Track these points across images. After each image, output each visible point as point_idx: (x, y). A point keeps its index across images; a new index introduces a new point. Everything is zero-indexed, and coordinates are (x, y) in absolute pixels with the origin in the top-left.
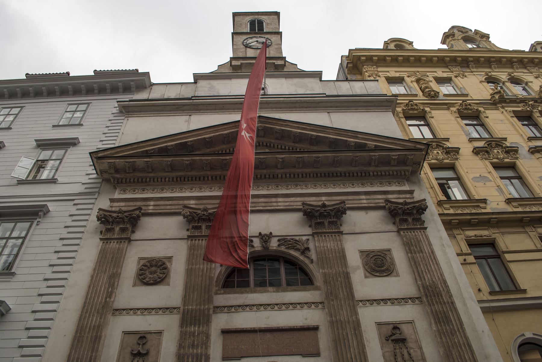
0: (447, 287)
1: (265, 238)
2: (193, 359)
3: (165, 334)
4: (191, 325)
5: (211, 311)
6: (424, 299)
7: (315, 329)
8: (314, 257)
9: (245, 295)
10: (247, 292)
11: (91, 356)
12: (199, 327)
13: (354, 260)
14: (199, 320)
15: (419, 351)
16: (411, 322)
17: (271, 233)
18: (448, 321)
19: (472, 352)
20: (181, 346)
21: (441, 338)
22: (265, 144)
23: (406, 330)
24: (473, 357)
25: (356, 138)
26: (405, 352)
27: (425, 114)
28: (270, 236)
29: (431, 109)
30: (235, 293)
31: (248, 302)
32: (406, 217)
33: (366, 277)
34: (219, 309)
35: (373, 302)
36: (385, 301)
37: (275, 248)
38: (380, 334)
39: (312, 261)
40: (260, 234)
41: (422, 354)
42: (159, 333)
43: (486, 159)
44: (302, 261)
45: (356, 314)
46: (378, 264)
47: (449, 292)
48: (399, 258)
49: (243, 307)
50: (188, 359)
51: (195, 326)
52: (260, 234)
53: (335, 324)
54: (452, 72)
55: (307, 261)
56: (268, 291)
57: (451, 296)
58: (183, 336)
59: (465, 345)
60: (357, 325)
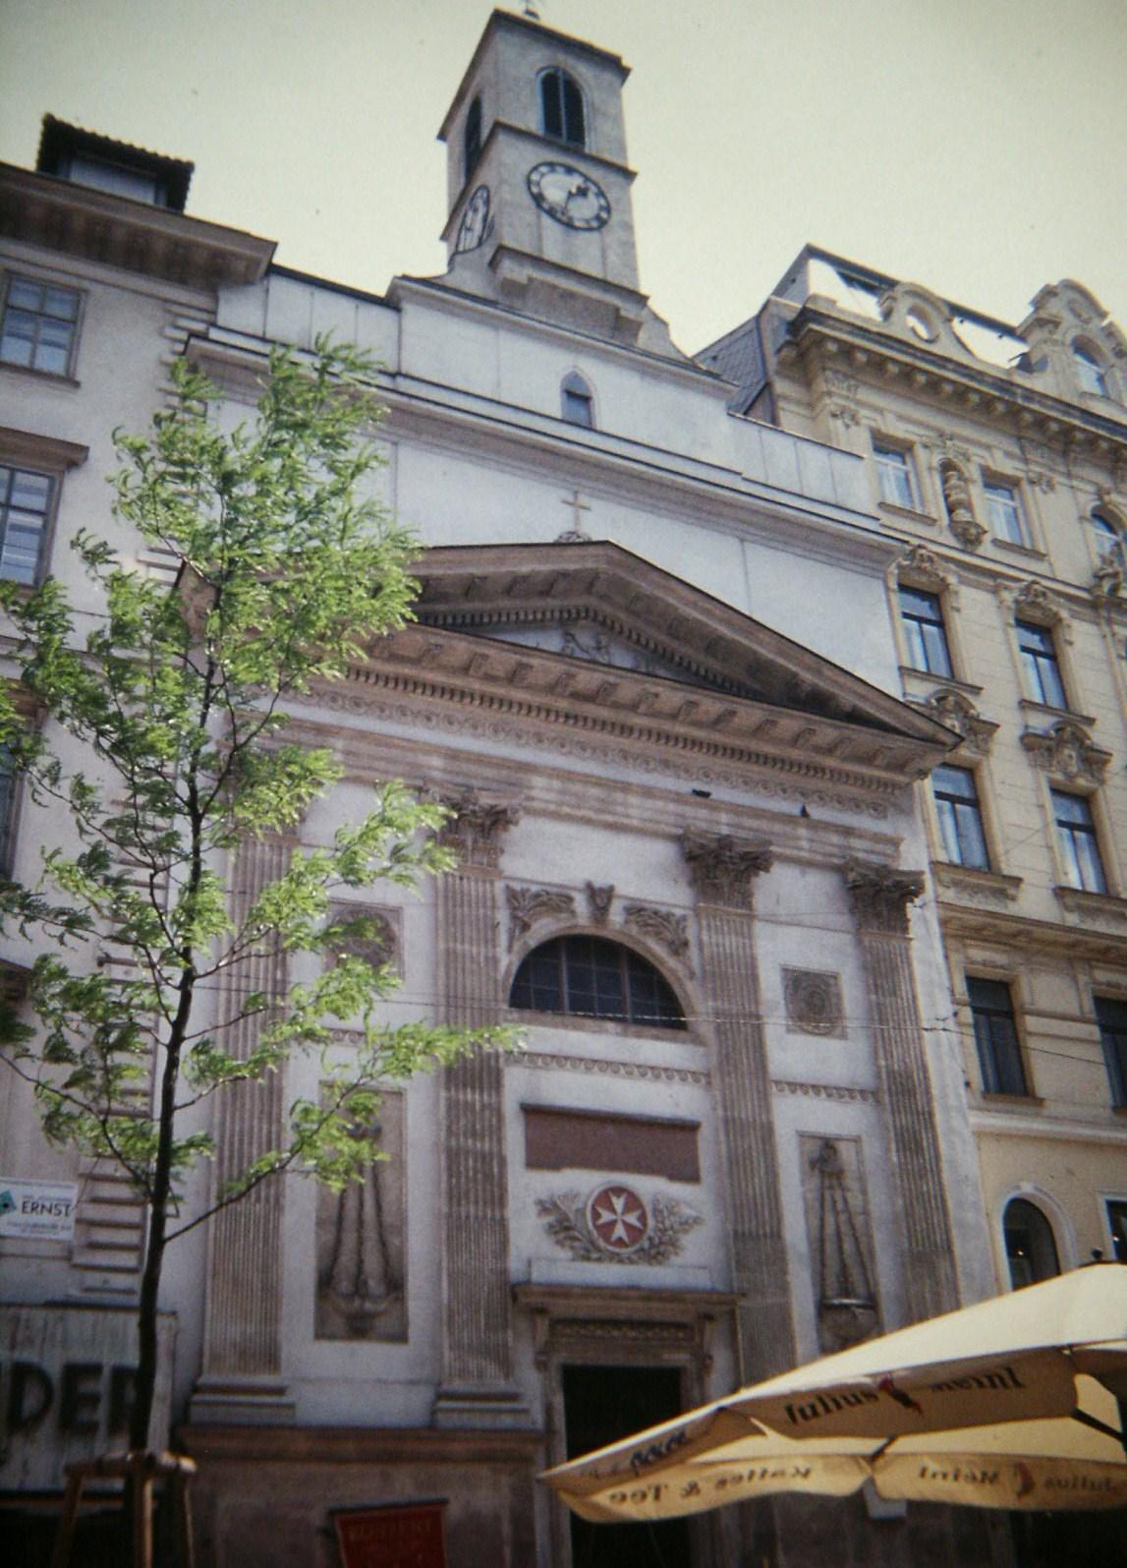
0: (926, 1078)
1: (600, 897)
2: (475, 1161)
4: (465, 1086)
5: (502, 1060)
6: (887, 1099)
8: (695, 963)
9: (562, 1032)
10: (566, 1027)
11: (270, 1132)
12: (481, 1095)
13: (771, 986)
14: (481, 1078)
15: (860, 1197)
16: (857, 1140)
17: (611, 889)
18: (918, 1149)
19: (945, 1214)
22: (600, 618)
23: (846, 1152)
25: (819, 673)
27: (943, 591)
28: (609, 893)
29: (962, 581)
30: (543, 1024)
31: (568, 1050)
32: (877, 898)
33: (789, 1031)
35: (795, 1087)
36: (816, 1089)
37: (617, 927)
38: (802, 1153)
39: (692, 975)
41: (866, 1202)
43: (1043, 767)
44: (673, 972)
45: (768, 1109)
46: (813, 1001)
47: (928, 1091)
48: (852, 995)
49: (559, 1060)
50: (466, 1160)
51: (473, 1088)
53: (731, 1125)
54: (1026, 461)
55: (681, 971)
56: (606, 1031)
57: (929, 1101)
60: (768, 1133)
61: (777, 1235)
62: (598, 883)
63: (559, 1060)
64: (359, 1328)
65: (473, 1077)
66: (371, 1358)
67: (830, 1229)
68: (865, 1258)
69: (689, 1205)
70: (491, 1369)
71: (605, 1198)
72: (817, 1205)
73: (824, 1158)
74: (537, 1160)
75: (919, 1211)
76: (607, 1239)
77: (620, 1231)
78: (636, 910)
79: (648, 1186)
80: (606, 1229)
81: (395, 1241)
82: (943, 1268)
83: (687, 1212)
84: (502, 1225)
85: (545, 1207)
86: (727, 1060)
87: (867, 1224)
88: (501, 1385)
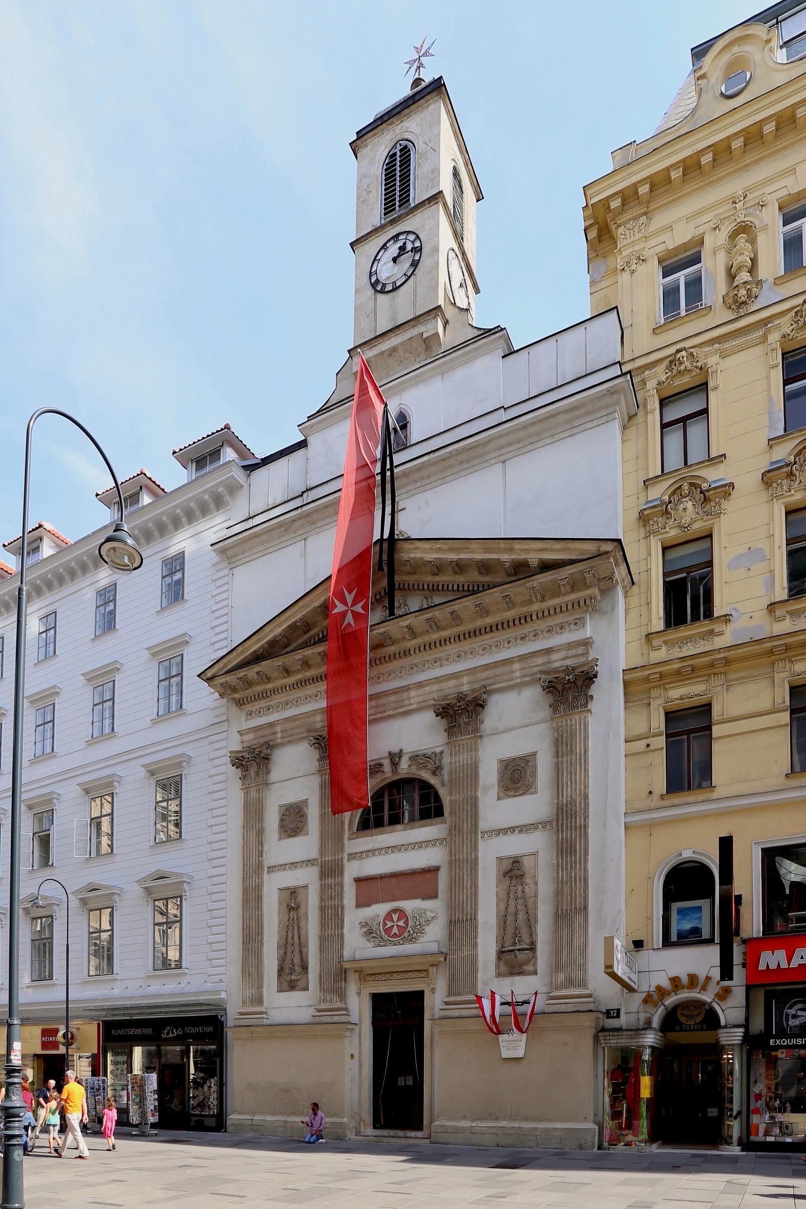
1: (395, 758)
3: (310, 888)
7: (436, 869)
16: (534, 854)
20: (322, 900)
21: (558, 873)
23: (527, 862)
24: (585, 893)
26: (520, 888)
31: (377, 846)
34: (352, 856)
36: (512, 829)
37: (406, 771)
40: (390, 753)
41: (537, 890)
42: (306, 887)
49: (372, 852)
52: (390, 753)
53: (454, 863)
56: (395, 831)
58: (323, 889)
59: (580, 880)
60: (474, 864)
61: (474, 919)
62: (396, 750)
63: (372, 852)
64: (292, 986)
65: (330, 871)
66: (296, 998)
67: (511, 909)
68: (531, 923)
69: (431, 911)
70: (336, 998)
71: (389, 916)
72: (505, 897)
73: (513, 871)
74: (359, 905)
75: (566, 890)
76: (389, 935)
77: (395, 930)
78: (414, 758)
79: (409, 905)
80: (388, 931)
81: (304, 950)
82: (579, 919)
83: (430, 915)
84: (342, 936)
85: (364, 924)
86: (454, 831)
87: (536, 903)
88: (339, 1005)
